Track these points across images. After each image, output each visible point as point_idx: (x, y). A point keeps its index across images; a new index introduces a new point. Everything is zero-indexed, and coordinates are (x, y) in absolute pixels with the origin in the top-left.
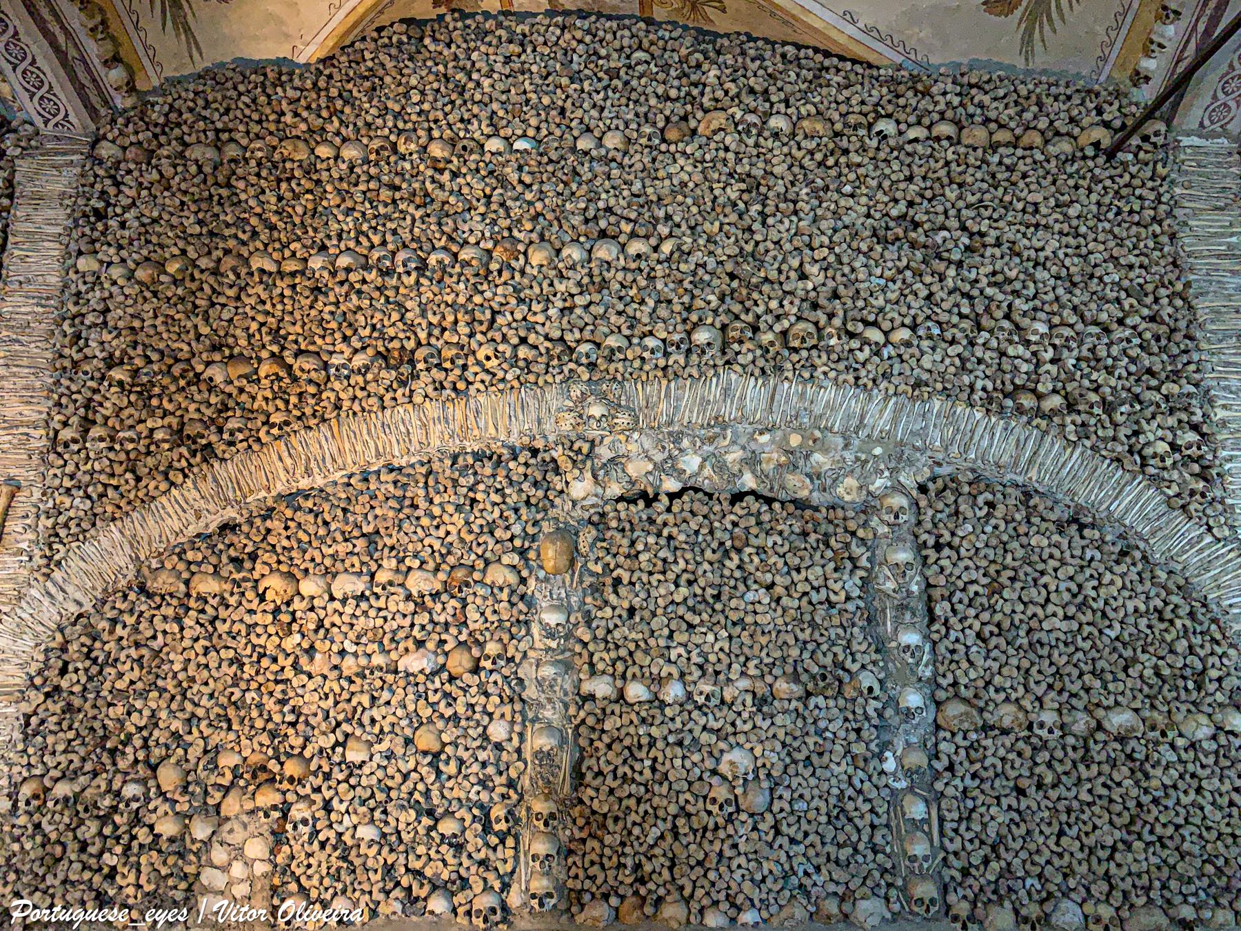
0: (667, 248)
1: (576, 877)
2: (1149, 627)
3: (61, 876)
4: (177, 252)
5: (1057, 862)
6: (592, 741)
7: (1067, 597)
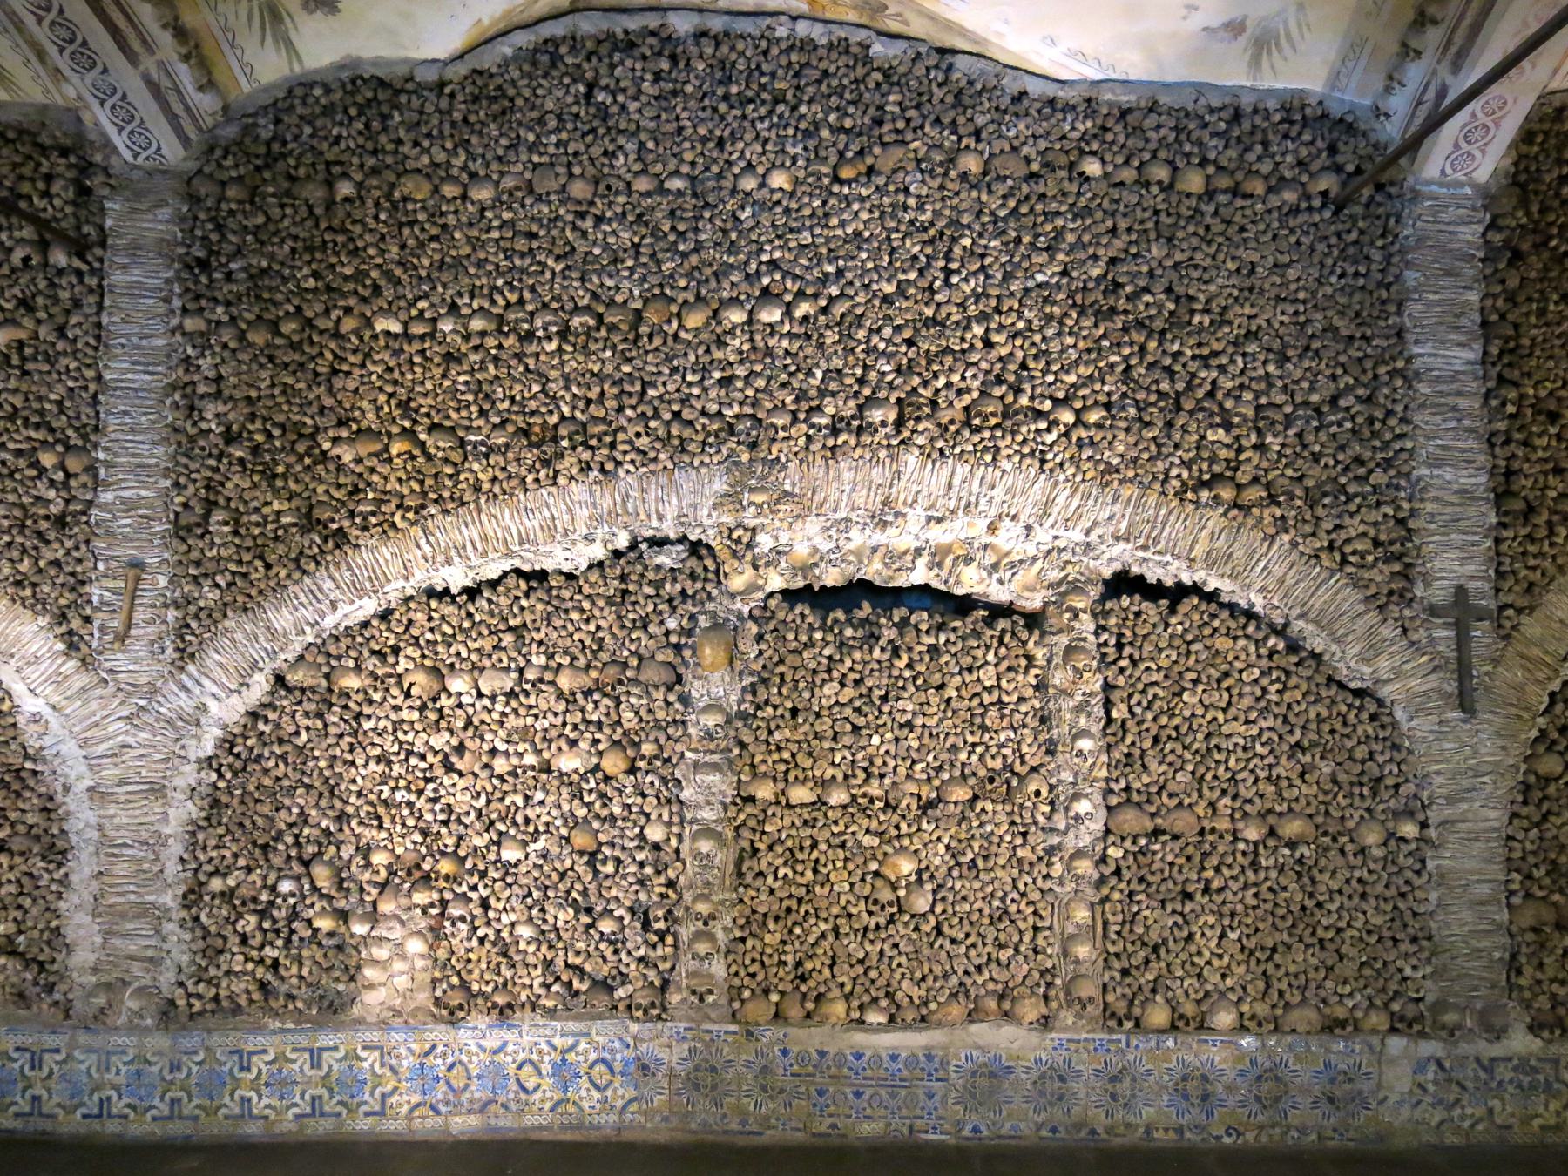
0: (839, 309)
3: (225, 967)
4: (292, 309)
5: (1216, 962)
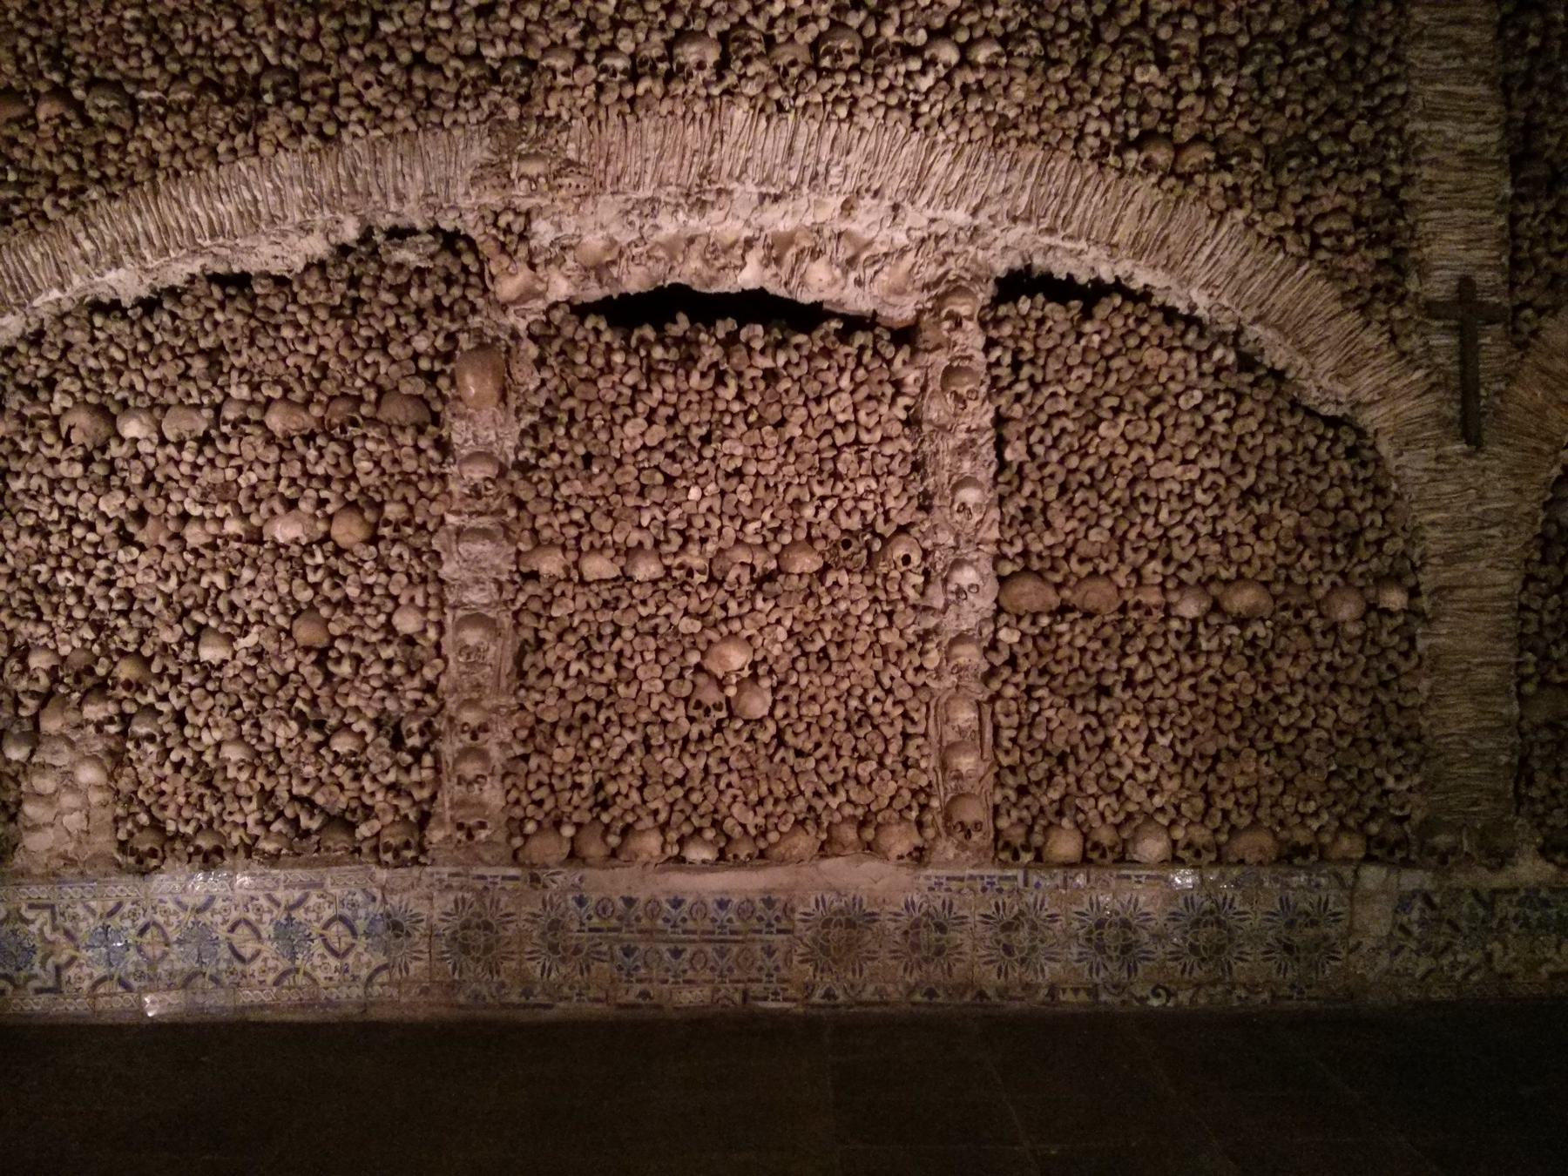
5: (1141, 776)
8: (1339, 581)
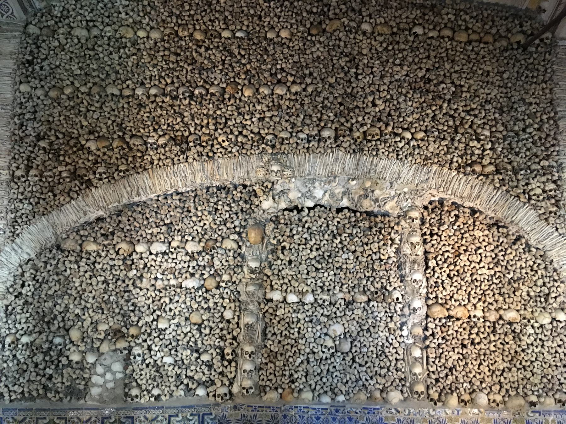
0: (310, 89)
1: (263, 380)
2: (527, 273)
3: (27, 378)
4: (69, 83)
5: (478, 376)
6: (271, 319)
7: (489, 259)
8: (543, 310)
